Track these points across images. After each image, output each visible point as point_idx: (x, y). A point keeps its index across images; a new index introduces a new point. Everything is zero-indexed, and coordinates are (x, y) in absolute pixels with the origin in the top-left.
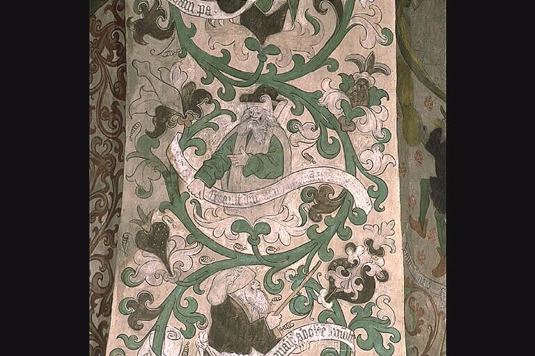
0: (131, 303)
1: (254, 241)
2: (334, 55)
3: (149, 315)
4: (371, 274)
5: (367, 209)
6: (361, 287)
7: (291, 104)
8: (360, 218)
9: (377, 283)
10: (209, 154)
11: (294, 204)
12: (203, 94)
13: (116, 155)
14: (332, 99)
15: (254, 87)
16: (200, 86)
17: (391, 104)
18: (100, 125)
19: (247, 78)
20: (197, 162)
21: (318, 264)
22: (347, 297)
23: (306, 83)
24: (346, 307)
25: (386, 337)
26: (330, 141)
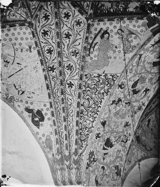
3: (99, 137)
4: (128, 139)
11: (124, 123)
13: (100, 103)
14: (136, 108)
22: (124, 142)
23: (134, 104)
24: (123, 143)
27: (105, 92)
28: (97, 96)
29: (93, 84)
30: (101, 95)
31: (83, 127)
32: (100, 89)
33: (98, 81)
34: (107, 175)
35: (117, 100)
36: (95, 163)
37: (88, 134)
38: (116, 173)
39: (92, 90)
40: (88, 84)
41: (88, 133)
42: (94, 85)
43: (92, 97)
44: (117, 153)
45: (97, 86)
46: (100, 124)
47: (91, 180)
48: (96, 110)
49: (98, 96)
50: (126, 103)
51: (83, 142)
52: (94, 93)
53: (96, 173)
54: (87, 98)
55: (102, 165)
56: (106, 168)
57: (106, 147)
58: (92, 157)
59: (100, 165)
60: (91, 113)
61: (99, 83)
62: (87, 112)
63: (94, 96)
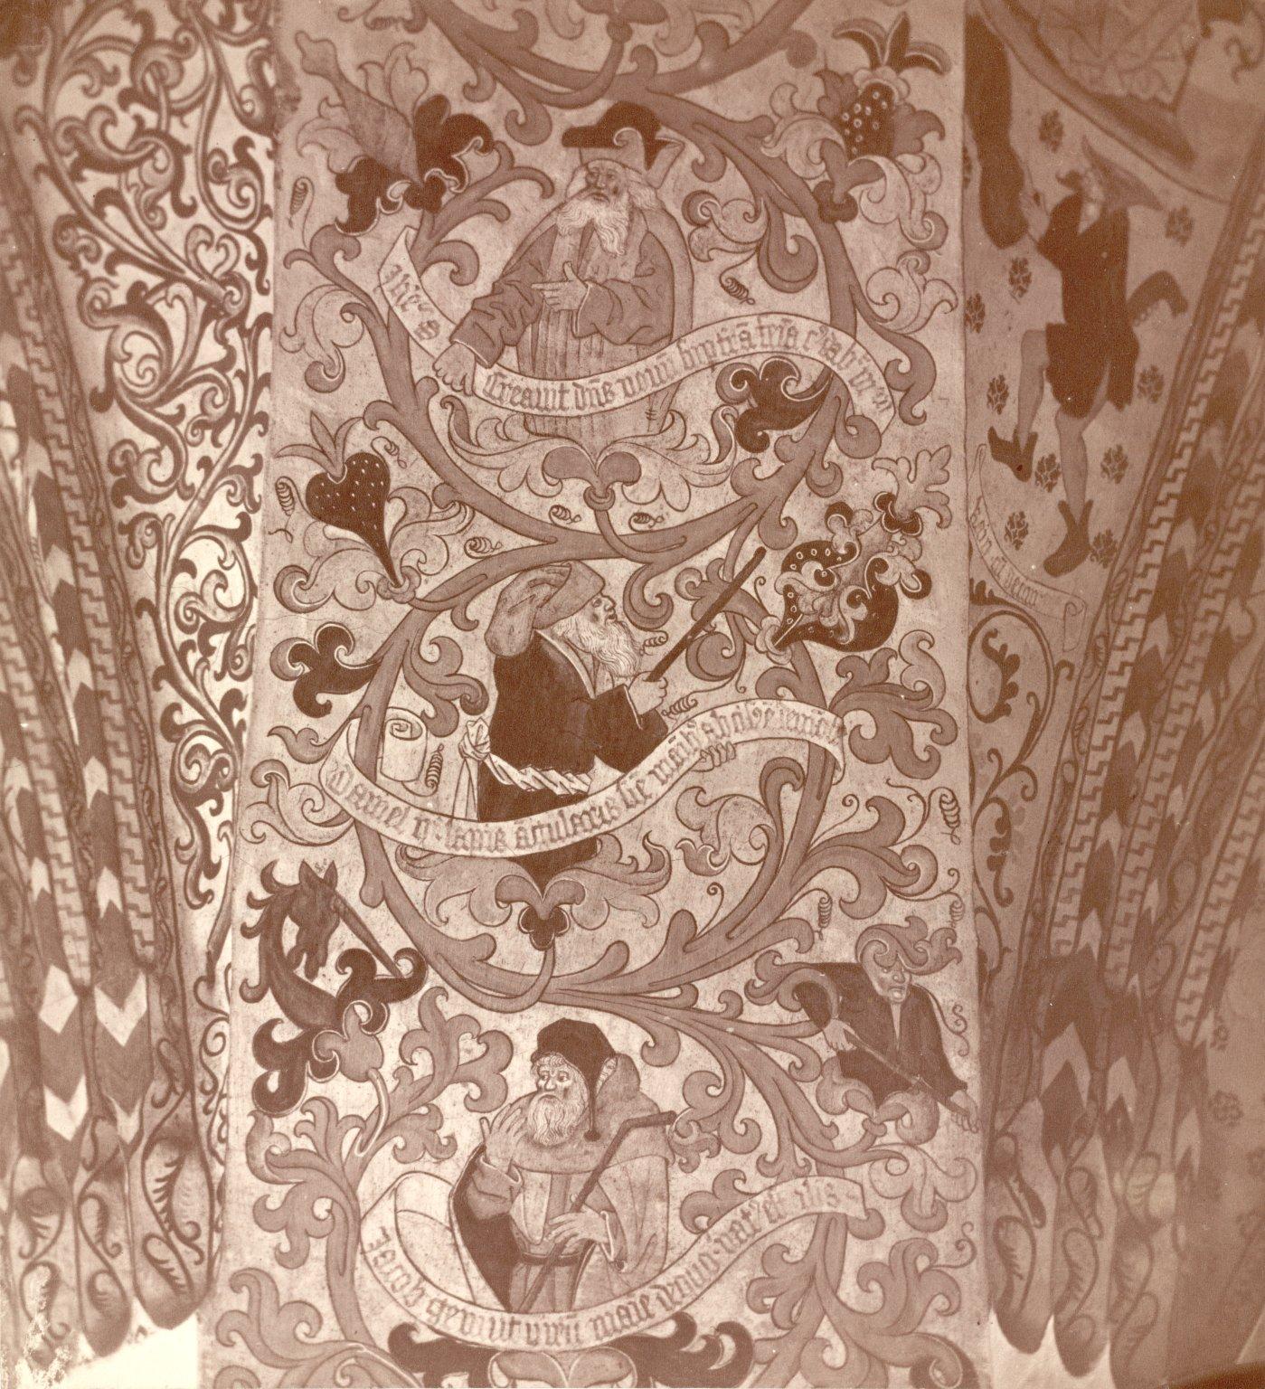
0: (300, 653)
1: (598, 500)
2: (802, 24)
4: (886, 579)
5: (883, 420)
6: (861, 612)
7: (693, 152)
8: (865, 438)
9: (905, 603)
10: (482, 287)
11: (700, 399)
12: (471, 127)
15: (602, 106)
16: (457, 107)
17: (952, 144)
18: (209, 198)
19: (580, 87)
20: (459, 303)
21: (760, 553)
22: (827, 637)
24: (824, 656)
25: (922, 733)
26: (792, 246)
27: (245, 119)
28: (203, 215)
29: (109, 96)
30: (234, 177)
31: (180, 637)
32: (193, 118)
33: (135, 33)
34: (671, 1116)
35: (400, 148)
36: (401, 1017)
37: (234, 700)
38: (850, 1065)
39: (133, 176)
40: (74, 129)
41: (228, 683)
42: (126, 98)
43: (163, 260)
44: (770, 804)
45: (152, 103)
46: (300, 520)
47: (370, 1233)
48: (242, 376)
49: (219, 214)
50: (573, 138)
51: (204, 810)
52: (165, 202)
53: (462, 1127)
54: (119, 298)
55: (541, 1017)
56: (623, 1035)
57: (524, 778)
58: (313, 948)
59: (509, 1025)
60: (207, 449)
61: (160, 54)
62: (167, 453)
63: (175, 231)
